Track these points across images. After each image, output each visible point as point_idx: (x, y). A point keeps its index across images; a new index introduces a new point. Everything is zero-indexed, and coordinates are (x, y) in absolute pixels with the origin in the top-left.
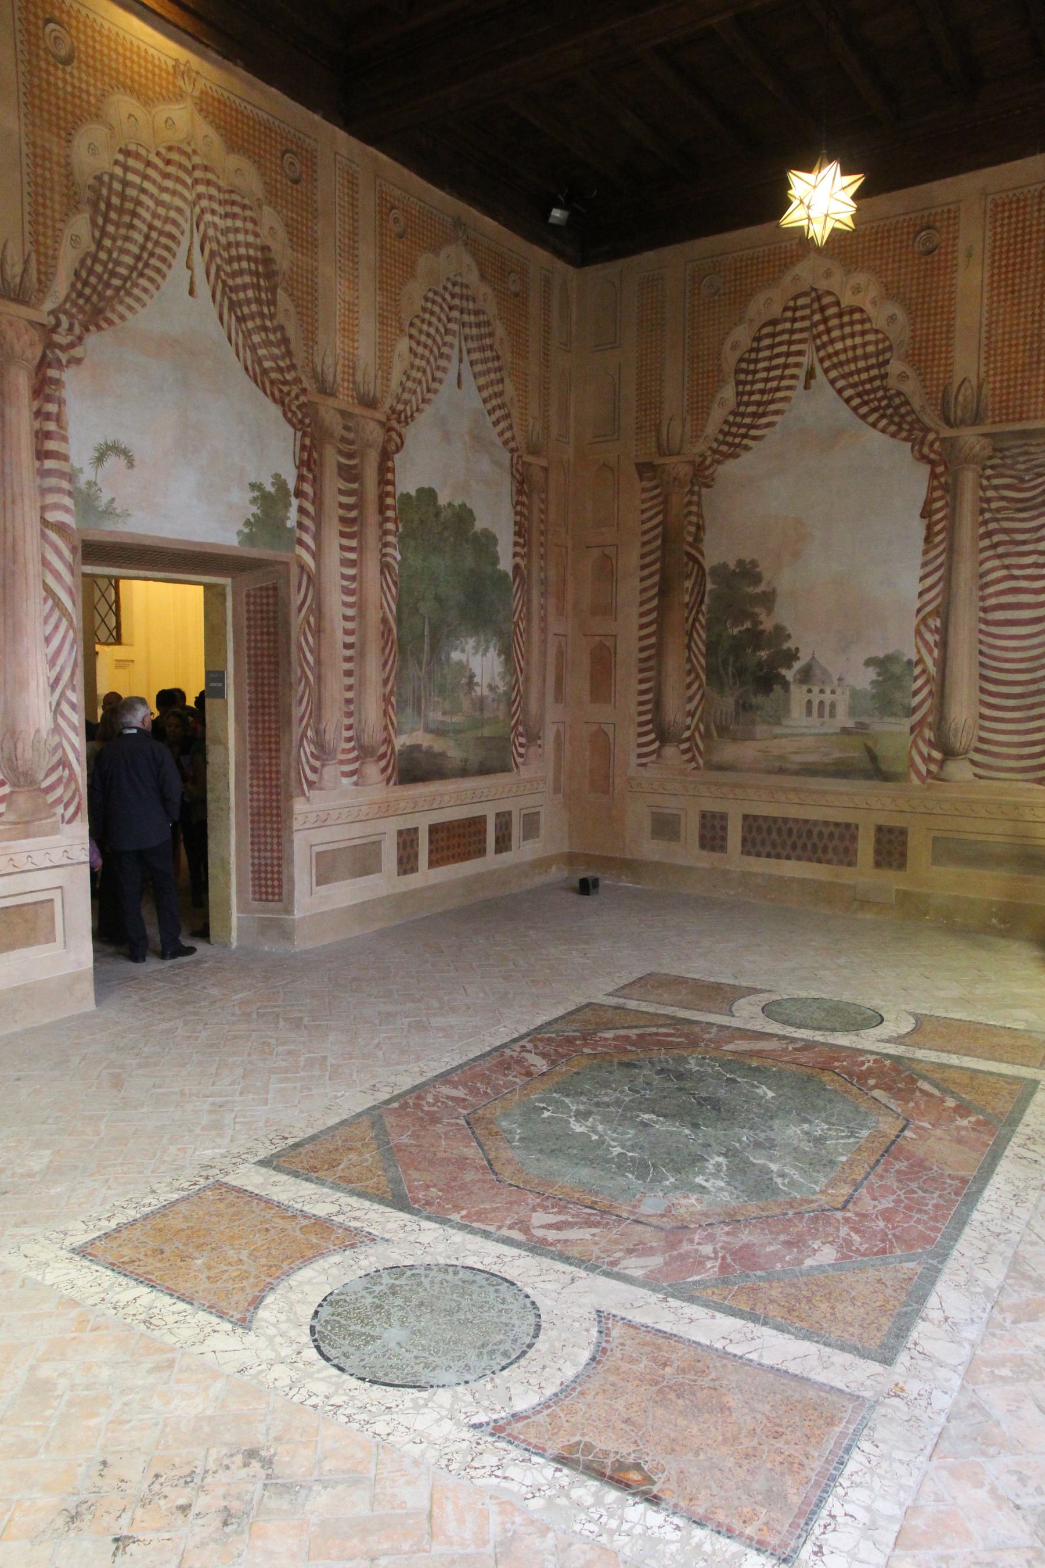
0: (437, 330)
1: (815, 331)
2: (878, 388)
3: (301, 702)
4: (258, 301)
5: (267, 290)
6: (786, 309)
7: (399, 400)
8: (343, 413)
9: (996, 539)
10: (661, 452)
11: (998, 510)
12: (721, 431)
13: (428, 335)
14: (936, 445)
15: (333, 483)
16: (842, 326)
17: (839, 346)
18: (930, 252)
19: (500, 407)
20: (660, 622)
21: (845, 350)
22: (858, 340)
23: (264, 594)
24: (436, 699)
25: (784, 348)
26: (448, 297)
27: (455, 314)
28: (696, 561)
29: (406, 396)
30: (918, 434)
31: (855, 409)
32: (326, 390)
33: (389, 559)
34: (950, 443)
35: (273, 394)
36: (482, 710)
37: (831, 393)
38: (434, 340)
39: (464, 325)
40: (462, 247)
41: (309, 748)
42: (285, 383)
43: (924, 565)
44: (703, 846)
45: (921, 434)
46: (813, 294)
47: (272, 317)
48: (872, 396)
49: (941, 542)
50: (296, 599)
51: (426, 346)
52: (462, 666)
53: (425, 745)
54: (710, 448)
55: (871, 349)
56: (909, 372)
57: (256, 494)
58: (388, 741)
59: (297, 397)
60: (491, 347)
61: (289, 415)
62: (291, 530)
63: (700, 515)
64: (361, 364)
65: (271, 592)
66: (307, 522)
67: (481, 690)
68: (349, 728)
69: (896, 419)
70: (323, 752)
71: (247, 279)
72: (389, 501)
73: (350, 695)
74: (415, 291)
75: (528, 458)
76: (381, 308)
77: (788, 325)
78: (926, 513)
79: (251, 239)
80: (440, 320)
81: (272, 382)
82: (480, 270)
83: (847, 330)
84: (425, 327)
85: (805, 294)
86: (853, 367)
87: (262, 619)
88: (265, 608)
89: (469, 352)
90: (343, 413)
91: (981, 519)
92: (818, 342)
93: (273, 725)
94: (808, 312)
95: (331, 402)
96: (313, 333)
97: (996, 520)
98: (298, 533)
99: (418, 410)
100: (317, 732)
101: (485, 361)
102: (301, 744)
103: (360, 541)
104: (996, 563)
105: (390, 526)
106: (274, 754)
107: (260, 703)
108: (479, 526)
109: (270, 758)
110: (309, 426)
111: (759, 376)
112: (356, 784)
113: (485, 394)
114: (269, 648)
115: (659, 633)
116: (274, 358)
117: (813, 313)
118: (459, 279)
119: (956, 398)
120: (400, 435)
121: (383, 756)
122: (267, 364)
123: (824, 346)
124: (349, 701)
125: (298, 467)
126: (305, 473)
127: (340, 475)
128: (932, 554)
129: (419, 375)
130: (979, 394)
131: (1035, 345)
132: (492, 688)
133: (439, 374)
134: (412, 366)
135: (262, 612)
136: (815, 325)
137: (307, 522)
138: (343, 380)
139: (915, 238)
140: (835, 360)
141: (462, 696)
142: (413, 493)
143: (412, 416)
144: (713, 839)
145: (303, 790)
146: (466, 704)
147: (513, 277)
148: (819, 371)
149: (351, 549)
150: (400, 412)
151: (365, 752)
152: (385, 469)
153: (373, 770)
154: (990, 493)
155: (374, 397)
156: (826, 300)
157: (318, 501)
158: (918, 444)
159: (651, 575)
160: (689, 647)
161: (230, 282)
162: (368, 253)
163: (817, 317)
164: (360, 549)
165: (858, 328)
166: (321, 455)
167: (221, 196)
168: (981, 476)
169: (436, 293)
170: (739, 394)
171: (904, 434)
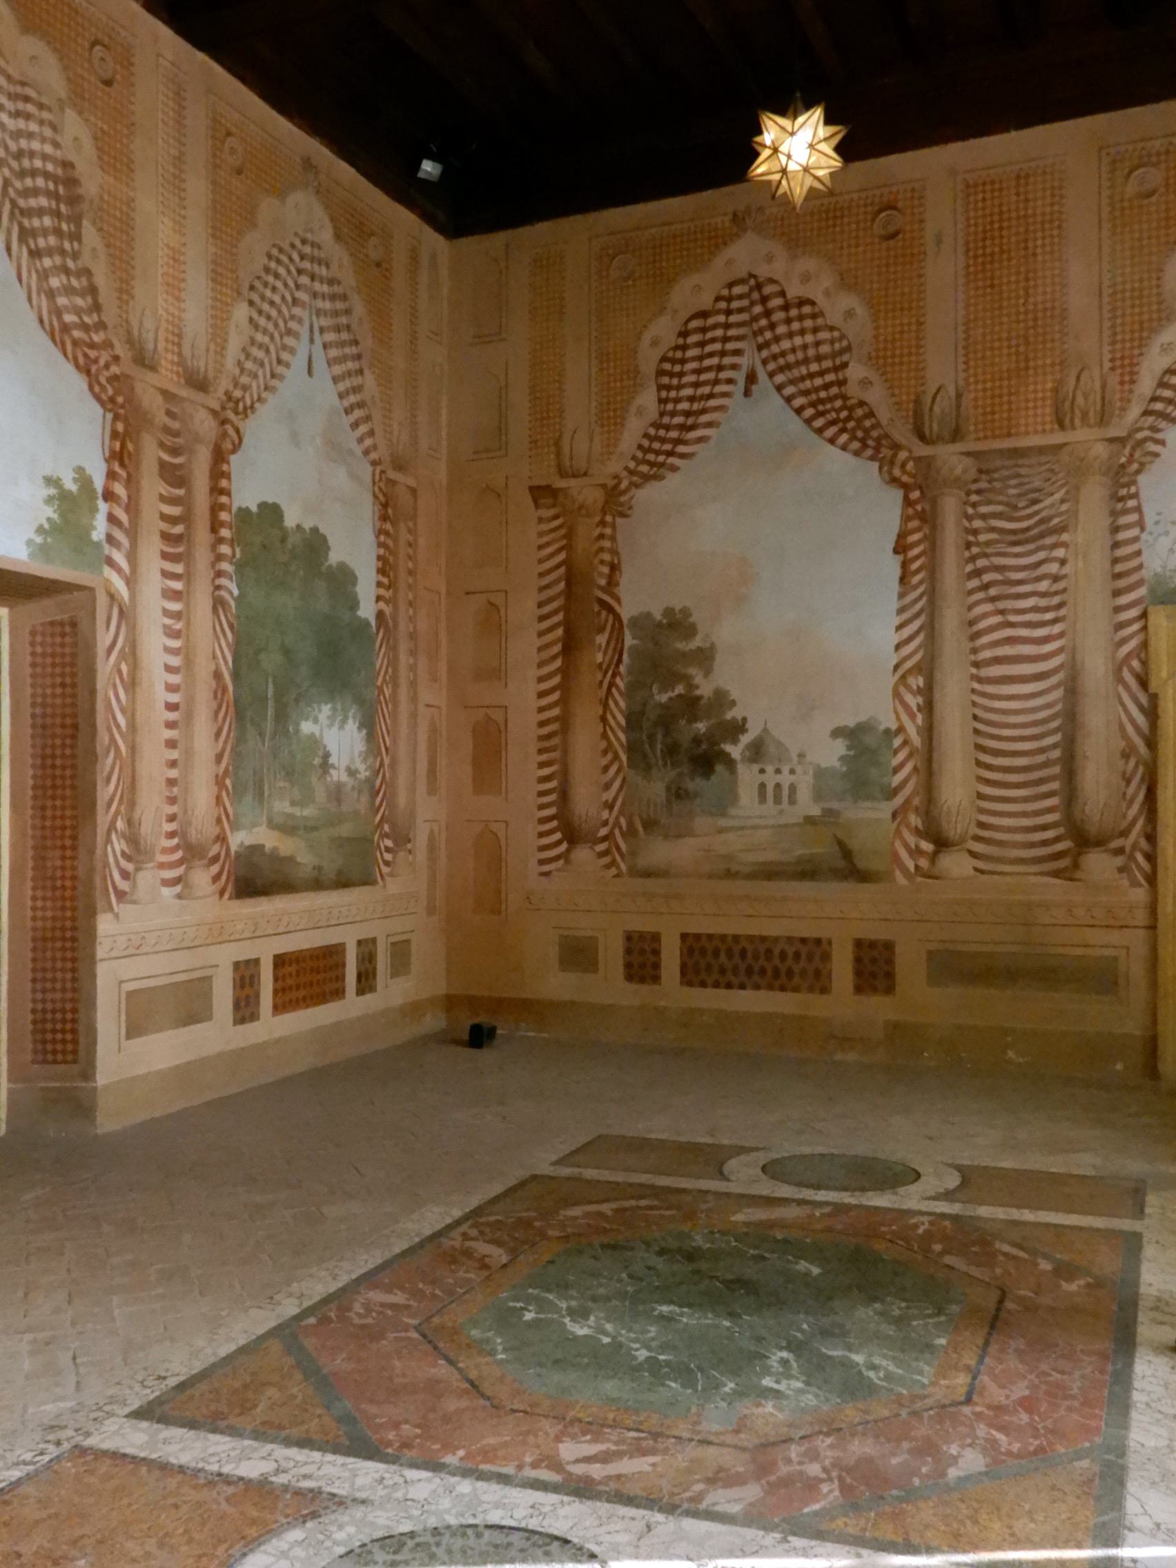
0: (283, 298)
1: (755, 326)
2: (836, 397)
3: (108, 780)
4: (58, 232)
5: (69, 219)
6: (718, 299)
7: (236, 385)
8: (166, 394)
9: (987, 578)
11: (988, 543)
12: (640, 447)
13: (272, 303)
14: (910, 466)
15: (152, 487)
16: (788, 321)
17: (786, 345)
18: (894, 236)
19: (360, 405)
21: (793, 350)
22: (809, 338)
23: (58, 630)
24: (282, 784)
25: (717, 346)
26: (295, 256)
27: (304, 280)
29: (244, 380)
30: (886, 452)
31: (808, 422)
32: (144, 361)
33: (223, 593)
34: (926, 464)
35: (75, 359)
36: (339, 801)
37: (778, 401)
38: (280, 312)
39: (315, 295)
40: (315, 194)
41: (118, 845)
42: (92, 346)
43: (901, 611)
44: (629, 978)
45: (890, 453)
46: (752, 282)
47: (75, 256)
48: (828, 406)
49: (921, 582)
50: (104, 639)
51: (269, 318)
52: (314, 743)
53: (269, 846)
54: (626, 468)
55: (825, 349)
56: (873, 376)
57: (52, 491)
58: (222, 839)
59: (107, 366)
60: (348, 327)
61: (97, 389)
62: (97, 545)
65: (68, 629)
66: (119, 535)
67: (338, 775)
68: (172, 818)
69: (860, 434)
70: (137, 850)
71: (43, 201)
72: (224, 516)
73: (173, 773)
74: (254, 249)
76: (214, 262)
77: (721, 318)
78: (900, 548)
79: (48, 149)
80: (286, 285)
81: (75, 343)
82: (335, 228)
83: (796, 326)
84: (268, 293)
85: (742, 281)
87: (54, 665)
88: (59, 650)
89: (322, 330)
90: (166, 394)
91: (967, 554)
92: (760, 339)
93: (68, 813)
94: (745, 303)
95: (150, 377)
96: (128, 283)
97: (986, 555)
98: (107, 549)
99: (259, 399)
100: (130, 822)
101: (342, 344)
102: (108, 840)
103: (187, 566)
105: (225, 549)
106: (68, 853)
107: (49, 782)
108: (334, 557)
109: (63, 858)
110: (122, 406)
111: (685, 380)
112: (179, 896)
114: (64, 705)
116: (78, 311)
117: (752, 304)
118: (309, 236)
119: (931, 409)
120: (238, 431)
121: (215, 859)
122: (69, 318)
123: (767, 345)
124: (171, 782)
125: (107, 461)
126: (117, 468)
127: (162, 476)
128: (908, 599)
129: (261, 354)
130: (958, 406)
131: (1022, 349)
132: (352, 772)
133: (285, 356)
134: (253, 341)
135: (53, 655)
136: (755, 319)
137: (119, 535)
138: (166, 350)
139: (873, 220)
140: (781, 361)
141: (314, 780)
142: (254, 509)
143: (252, 407)
145: (109, 903)
146: (320, 795)
147: (374, 240)
148: (762, 375)
149: (176, 577)
150: (237, 402)
151: (192, 852)
152: (218, 472)
153: (202, 878)
154: (978, 524)
155: (205, 378)
156: (768, 290)
157: (132, 507)
158: (886, 464)
161: (21, 202)
162: (198, 189)
163: (758, 309)
164: (186, 577)
165: (808, 323)
166: (138, 449)
167: (12, 89)
169: (281, 250)
171: (869, 452)
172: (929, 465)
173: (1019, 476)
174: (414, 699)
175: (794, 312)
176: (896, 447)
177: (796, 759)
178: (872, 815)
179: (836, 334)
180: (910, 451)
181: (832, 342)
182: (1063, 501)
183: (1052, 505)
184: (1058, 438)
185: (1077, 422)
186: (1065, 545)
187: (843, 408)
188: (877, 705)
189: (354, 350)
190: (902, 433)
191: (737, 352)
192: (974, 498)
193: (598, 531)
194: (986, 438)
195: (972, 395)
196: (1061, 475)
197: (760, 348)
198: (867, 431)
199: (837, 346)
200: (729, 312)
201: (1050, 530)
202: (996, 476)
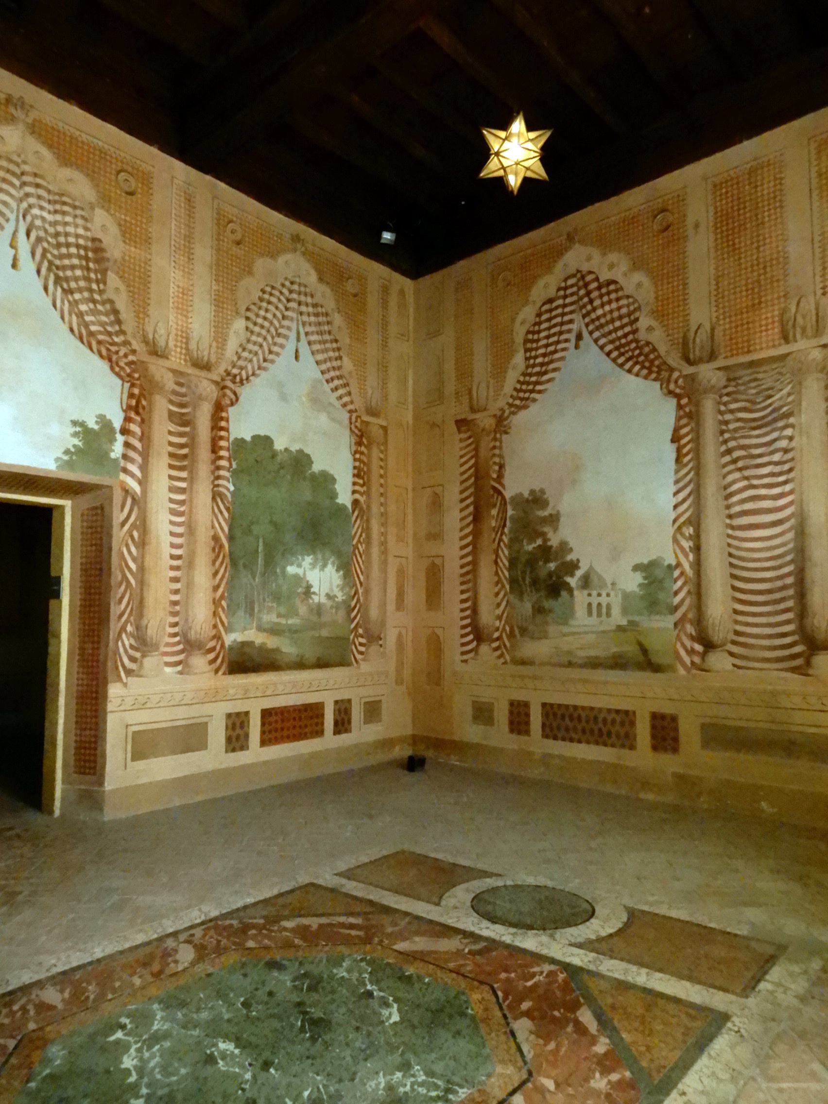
1: (581, 303)
2: (631, 341)
9: (736, 454)
10: (473, 410)
11: (736, 430)
14: (680, 381)
16: (601, 296)
17: (600, 312)
20: (474, 544)
21: (604, 315)
22: (614, 305)
25: (559, 320)
28: (499, 493)
29: (241, 363)
31: (614, 360)
32: (156, 352)
42: (113, 344)
43: (677, 482)
46: (579, 275)
49: (690, 461)
56: (654, 323)
59: (126, 356)
63: (501, 456)
64: (195, 336)
69: (647, 364)
75: (366, 418)
77: (560, 302)
81: (99, 343)
83: (605, 299)
86: (611, 327)
91: (721, 439)
94: (575, 289)
95: (161, 362)
97: (735, 439)
104: (737, 475)
113: (324, 367)
115: (474, 552)
117: (579, 289)
123: (588, 314)
129: (256, 348)
136: (581, 299)
138: (176, 346)
140: (597, 323)
144: (519, 723)
148: (585, 334)
154: (728, 417)
159: (467, 506)
160: (496, 563)
168: (719, 403)
170: (527, 359)
171: (654, 376)
172: (693, 380)
173: (756, 380)
174: (384, 552)
175: (604, 290)
176: (671, 370)
177: (610, 586)
178: (662, 625)
179: (631, 300)
180: (680, 371)
181: (628, 306)
182: (789, 394)
183: (780, 399)
184: (784, 349)
185: (798, 336)
186: (792, 426)
187: (637, 348)
188: (663, 548)
189: (335, 345)
190: (674, 359)
192: (725, 399)
193: (492, 444)
194: (732, 356)
195: (722, 328)
196: (788, 375)
197: (584, 317)
198: (652, 362)
199: (632, 308)
200: (565, 297)
201: (781, 417)
202: (740, 382)
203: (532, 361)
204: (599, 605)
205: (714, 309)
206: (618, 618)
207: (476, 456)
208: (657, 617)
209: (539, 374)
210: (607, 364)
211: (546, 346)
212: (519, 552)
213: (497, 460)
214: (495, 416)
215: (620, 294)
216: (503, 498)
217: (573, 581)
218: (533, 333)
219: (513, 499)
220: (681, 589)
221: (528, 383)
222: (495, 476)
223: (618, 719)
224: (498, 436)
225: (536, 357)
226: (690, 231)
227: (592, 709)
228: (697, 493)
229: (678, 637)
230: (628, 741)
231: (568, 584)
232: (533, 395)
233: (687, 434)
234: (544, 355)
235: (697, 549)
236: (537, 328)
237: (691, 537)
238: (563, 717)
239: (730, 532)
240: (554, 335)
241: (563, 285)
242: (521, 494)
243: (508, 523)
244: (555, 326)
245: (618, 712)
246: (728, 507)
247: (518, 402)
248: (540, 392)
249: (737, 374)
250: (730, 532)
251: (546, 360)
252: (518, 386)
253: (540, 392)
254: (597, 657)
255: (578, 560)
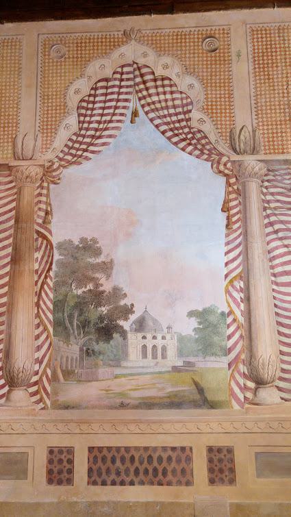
2: (185, 127)
9: (277, 227)
11: (275, 208)
14: (229, 165)
16: (156, 87)
17: (155, 98)
21: (160, 102)
22: (168, 96)
31: (169, 138)
43: (227, 244)
45: (217, 157)
46: (135, 66)
48: (181, 131)
49: (239, 228)
55: (178, 102)
77: (117, 83)
83: (160, 90)
85: (129, 65)
91: (264, 214)
92: (140, 95)
94: (131, 76)
97: (276, 215)
117: (135, 77)
123: (144, 97)
128: (232, 237)
136: (138, 84)
154: (269, 197)
156: (144, 70)
165: (168, 89)
168: (261, 186)
175: (159, 83)
176: (221, 155)
177: (166, 330)
179: (184, 96)
180: (229, 158)
181: (182, 99)
188: (216, 296)
190: (223, 147)
191: (126, 100)
192: (266, 184)
194: (270, 153)
195: (261, 132)
197: (140, 99)
199: (185, 102)
200: (122, 80)
203: (86, 125)
204: (154, 347)
205: (254, 117)
206: (173, 360)
207: (18, 200)
208: (213, 358)
209: (93, 137)
210: (162, 140)
211: (102, 115)
212: (66, 296)
213: (43, 206)
214: (43, 166)
215: (174, 89)
216: (49, 242)
217: (126, 325)
218: (88, 102)
219: (60, 246)
220: (233, 334)
221: (81, 143)
222: (40, 221)
223: (174, 455)
224: (45, 184)
225: (90, 122)
226: (234, 58)
227: (146, 449)
228: (246, 253)
229: (232, 376)
230: (185, 478)
231: (122, 327)
232: (85, 154)
233: (236, 206)
234: (99, 122)
235: (248, 299)
236: (92, 99)
237: (241, 290)
238: (113, 461)
239: (275, 287)
240: (109, 108)
241: (119, 70)
242: (70, 241)
243: (54, 266)
244: (111, 100)
245: (174, 449)
246: (272, 267)
247: (69, 158)
248: (93, 152)
249: (277, 167)
250: (275, 287)
251: (101, 126)
252: (70, 144)
253: (93, 152)
254: (150, 398)
255: (132, 305)
